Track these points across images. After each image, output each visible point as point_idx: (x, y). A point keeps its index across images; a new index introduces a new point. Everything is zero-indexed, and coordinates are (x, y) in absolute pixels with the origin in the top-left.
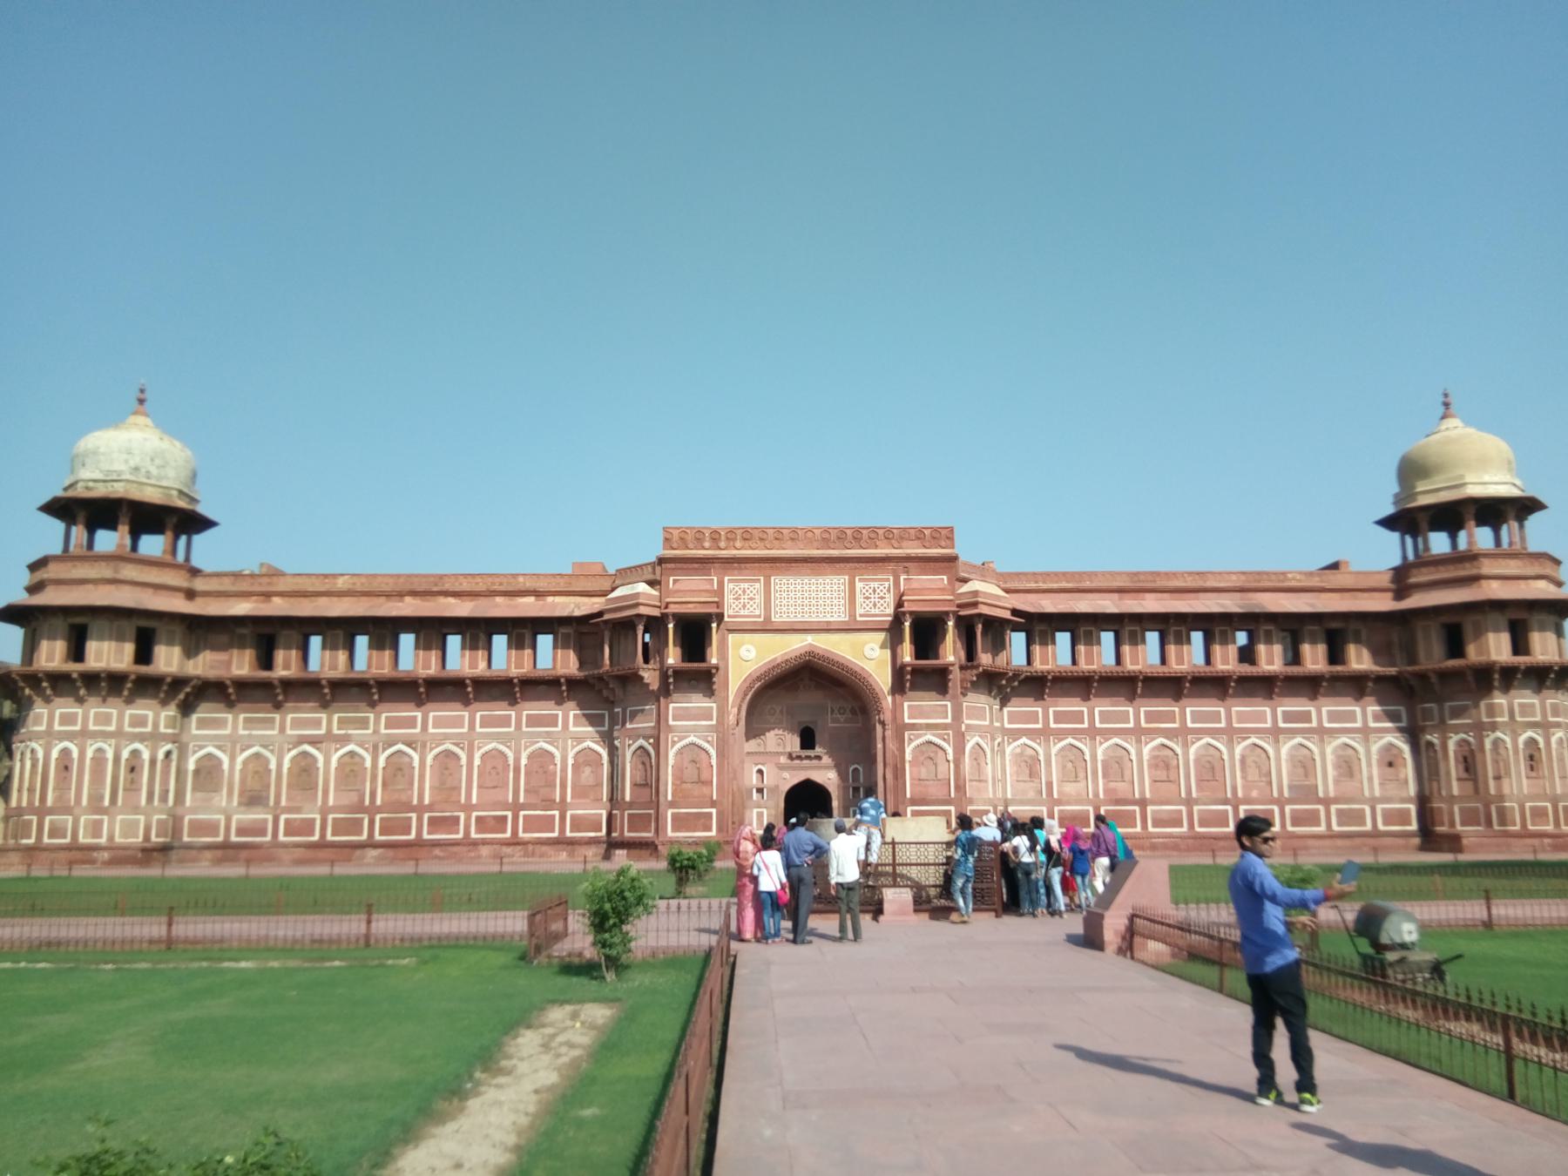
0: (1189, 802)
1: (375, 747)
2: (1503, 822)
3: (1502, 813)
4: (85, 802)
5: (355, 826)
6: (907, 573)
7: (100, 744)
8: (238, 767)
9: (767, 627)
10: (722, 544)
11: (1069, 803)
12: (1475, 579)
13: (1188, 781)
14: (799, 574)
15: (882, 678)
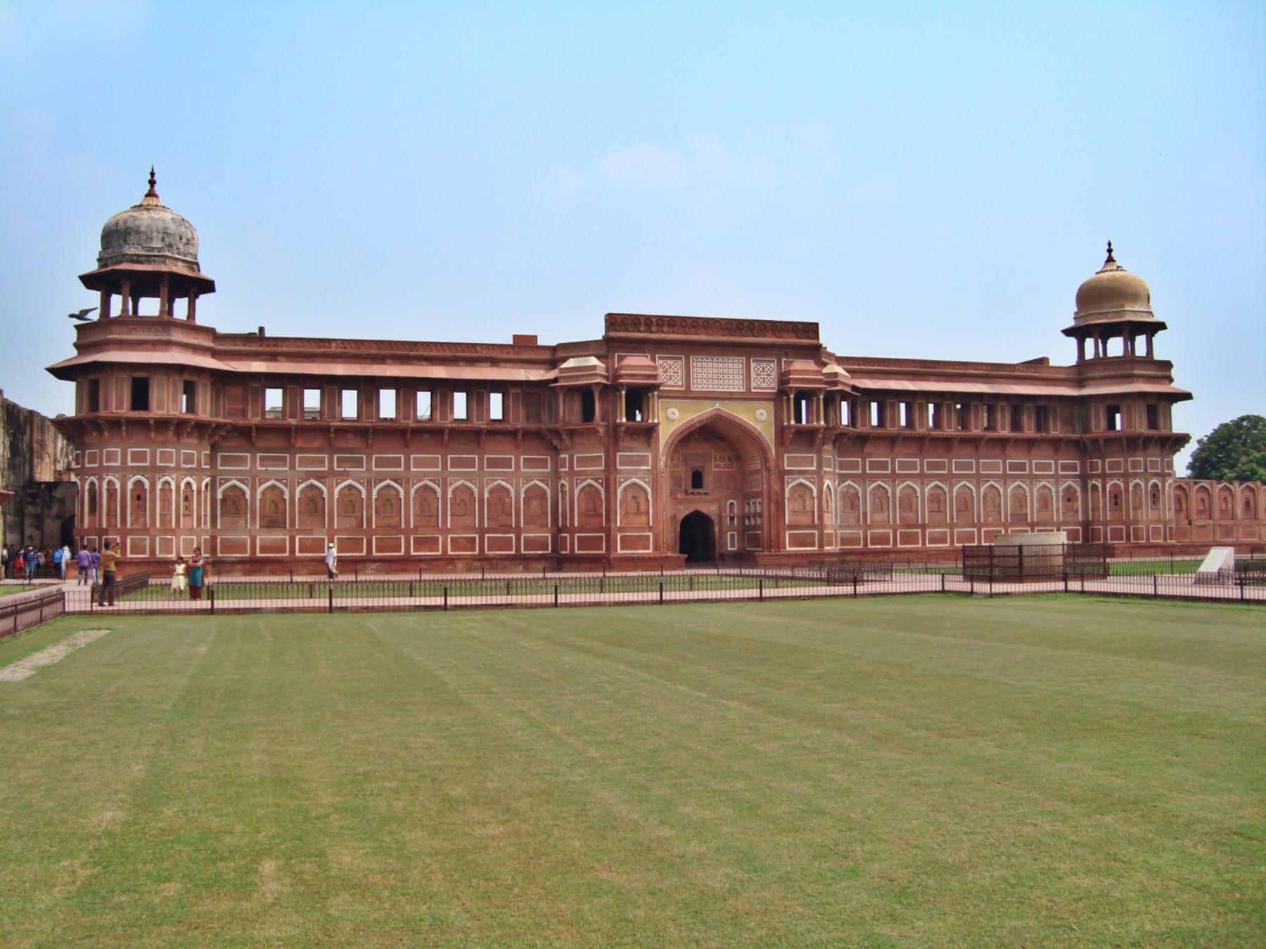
1: (369, 482)
2: (1136, 538)
3: (1136, 531)
4: (158, 525)
5: (356, 545)
6: (786, 356)
8: (258, 497)
9: (687, 395)
10: (654, 329)
11: (877, 528)
12: (1131, 378)
13: (951, 510)
14: (710, 354)
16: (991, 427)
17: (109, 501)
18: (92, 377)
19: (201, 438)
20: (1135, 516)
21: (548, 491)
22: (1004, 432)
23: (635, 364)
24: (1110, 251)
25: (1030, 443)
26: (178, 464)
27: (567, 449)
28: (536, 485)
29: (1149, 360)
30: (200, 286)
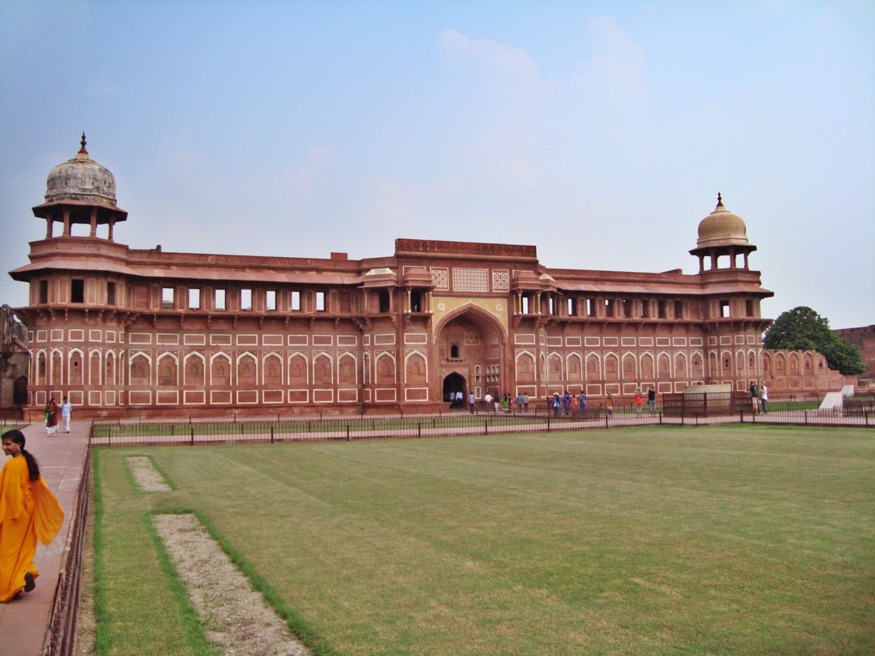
0: (621, 381)
1: (234, 354)
2: (740, 388)
4: (90, 383)
5: (225, 397)
6: (516, 268)
7: (96, 350)
8: (158, 364)
9: (450, 294)
10: (428, 249)
11: (573, 383)
12: (736, 282)
13: (620, 372)
15: (503, 320)
16: (645, 315)
17: (55, 366)
18: (43, 279)
19: (119, 323)
20: (740, 373)
21: (356, 360)
22: (654, 318)
23: (416, 274)
24: (720, 199)
25: (670, 326)
26: (104, 340)
27: (370, 330)
28: (347, 356)
29: (746, 271)
30: (113, 216)
